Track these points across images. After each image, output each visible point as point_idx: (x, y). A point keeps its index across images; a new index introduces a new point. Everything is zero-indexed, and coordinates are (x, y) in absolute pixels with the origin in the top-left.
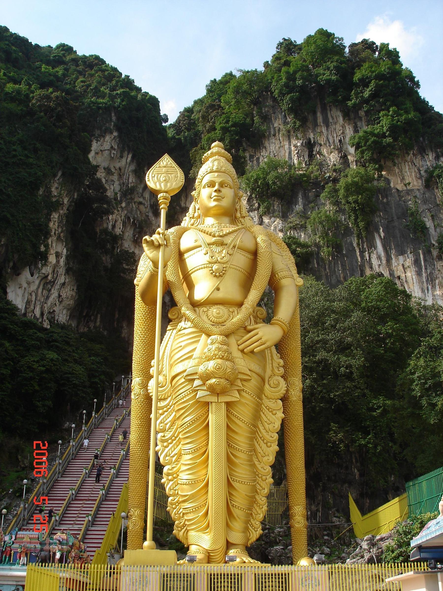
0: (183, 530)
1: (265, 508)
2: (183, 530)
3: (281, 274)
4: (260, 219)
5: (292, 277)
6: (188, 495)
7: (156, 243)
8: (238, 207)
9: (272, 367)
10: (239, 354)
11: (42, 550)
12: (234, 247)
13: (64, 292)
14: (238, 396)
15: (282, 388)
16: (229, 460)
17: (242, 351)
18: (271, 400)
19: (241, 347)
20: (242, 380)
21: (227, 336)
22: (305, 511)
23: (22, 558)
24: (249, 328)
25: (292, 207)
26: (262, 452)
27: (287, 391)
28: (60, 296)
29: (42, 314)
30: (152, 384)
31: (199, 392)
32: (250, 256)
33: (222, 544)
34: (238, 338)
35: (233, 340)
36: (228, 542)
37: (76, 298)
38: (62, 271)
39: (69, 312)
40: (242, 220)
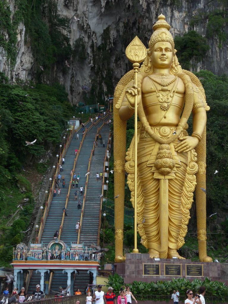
0: (145, 242)
1: (186, 231)
2: (145, 242)
3: (198, 105)
4: (171, 13)
5: (204, 106)
6: (149, 225)
7: (134, 94)
8: (173, 60)
9: (191, 157)
10: (175, 153)
11: (84, 253)
12: (174, 92)
13: (24, 58)
14: (175, 176)
15: (196, 169)
16: (169, 208)
17: (177, 152)
18: (190, 175)
19: (177, 150)
20: (177, 167)
21: (169, 144)
22: (206, 232)
23: (76, 257)
24: (181, 138)
25: (195, 5)
26: (185, 203)
27: (198, 170)
28: (21, 62)
29: (12, 78)
30: (127, 165)
31: (155, 174)
32: (180, 96)
33: (166, 249)
34: (175, 144)
35: (172, 145)
36: (169, 248)
37: (33, 62)
38: (22, 43)
39: (27, 72)
40: (176, 68)
